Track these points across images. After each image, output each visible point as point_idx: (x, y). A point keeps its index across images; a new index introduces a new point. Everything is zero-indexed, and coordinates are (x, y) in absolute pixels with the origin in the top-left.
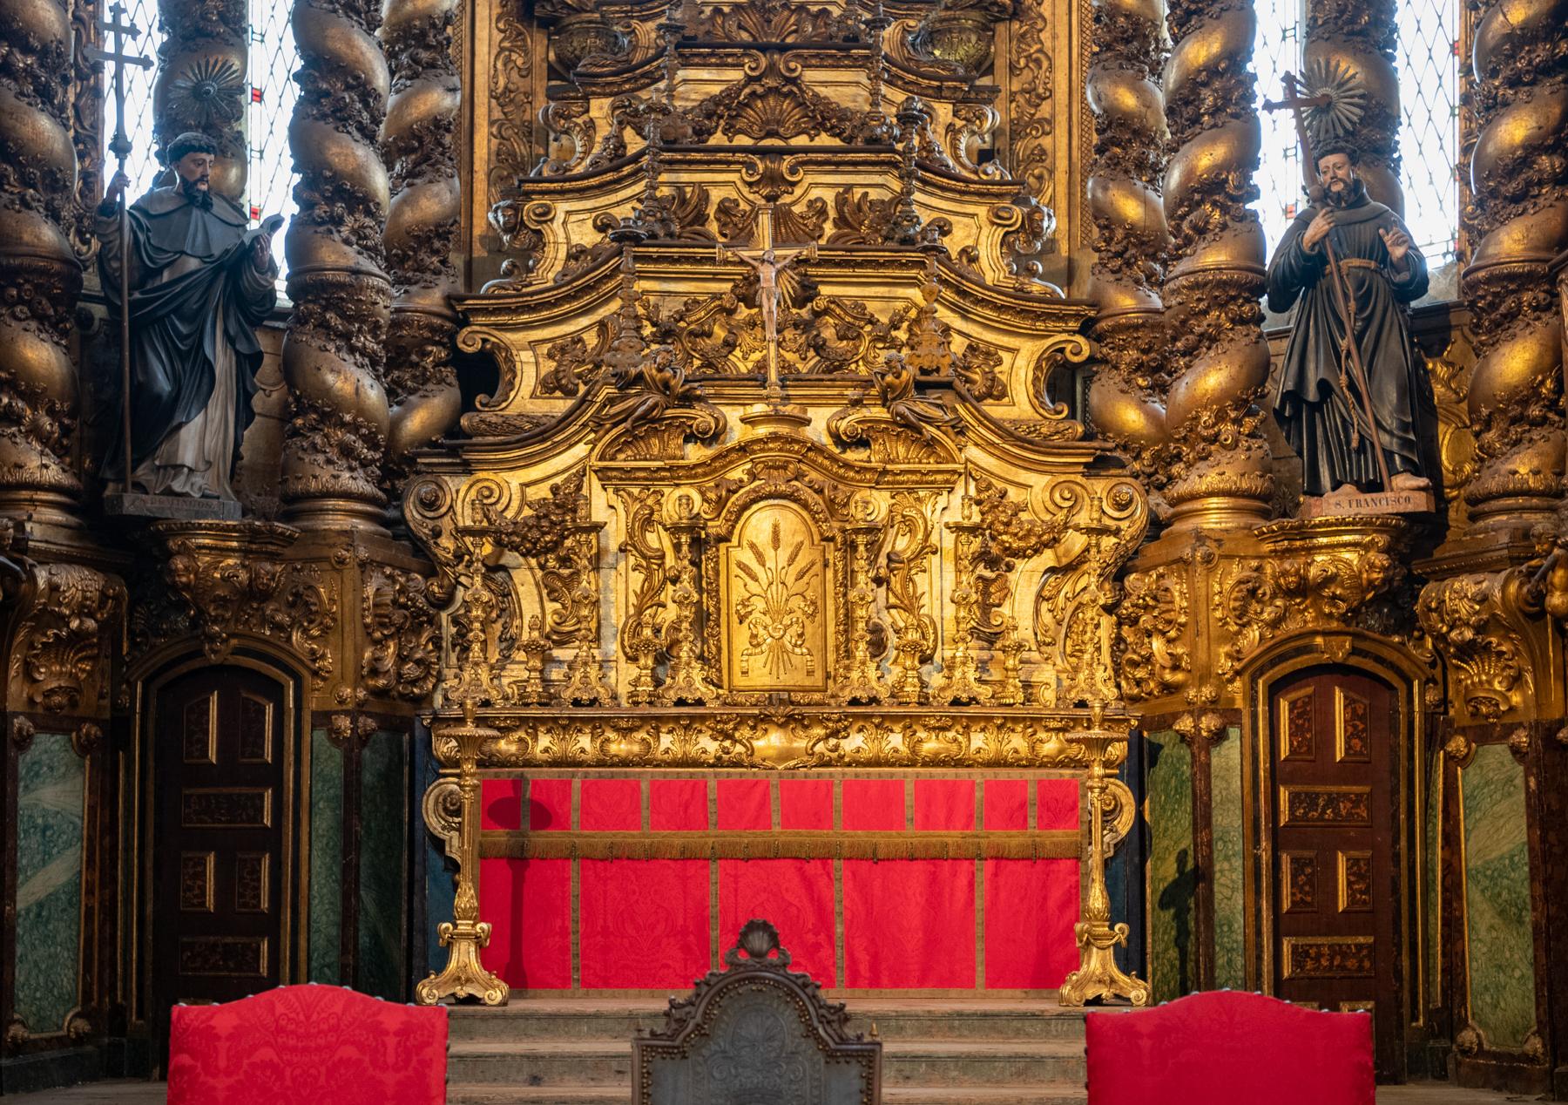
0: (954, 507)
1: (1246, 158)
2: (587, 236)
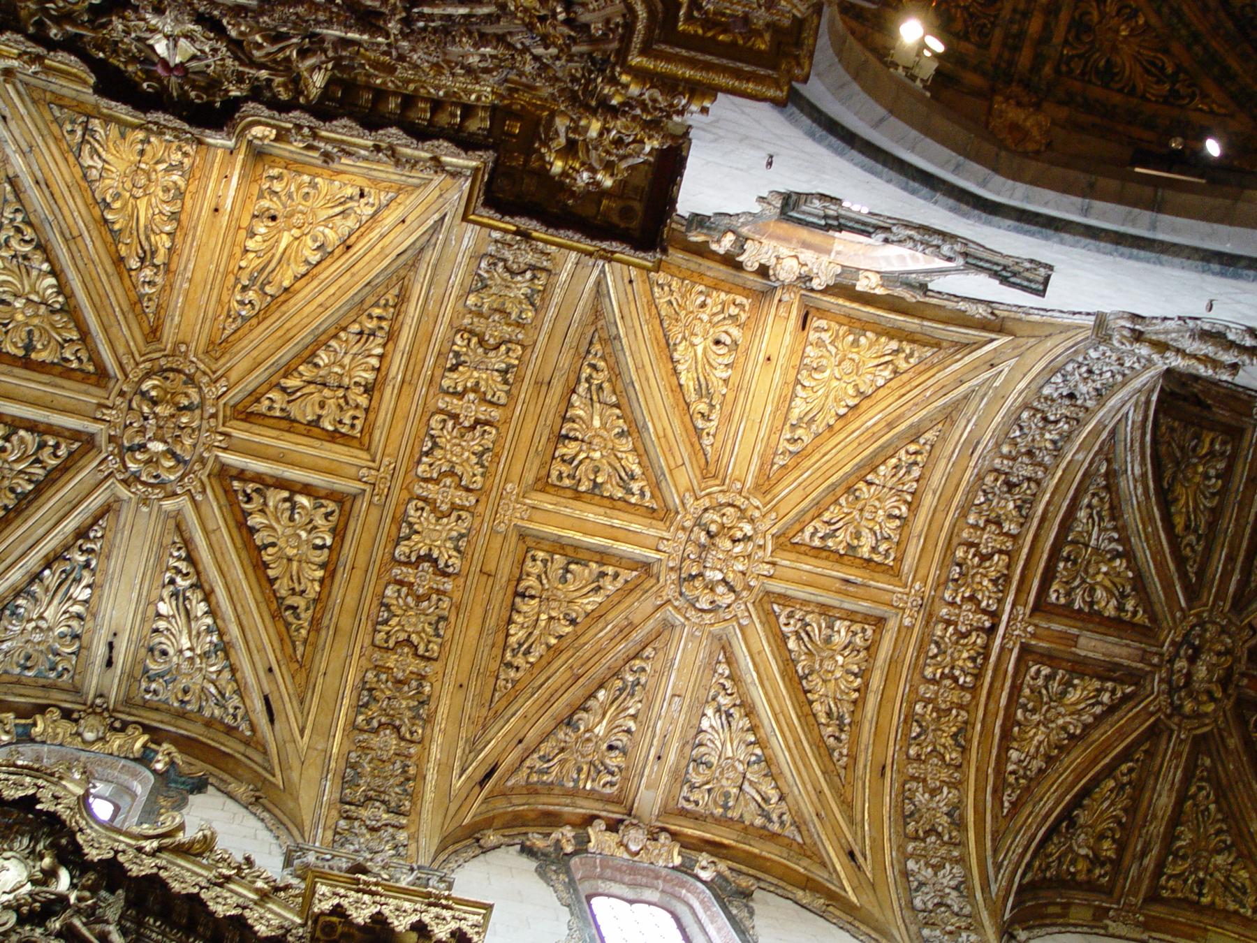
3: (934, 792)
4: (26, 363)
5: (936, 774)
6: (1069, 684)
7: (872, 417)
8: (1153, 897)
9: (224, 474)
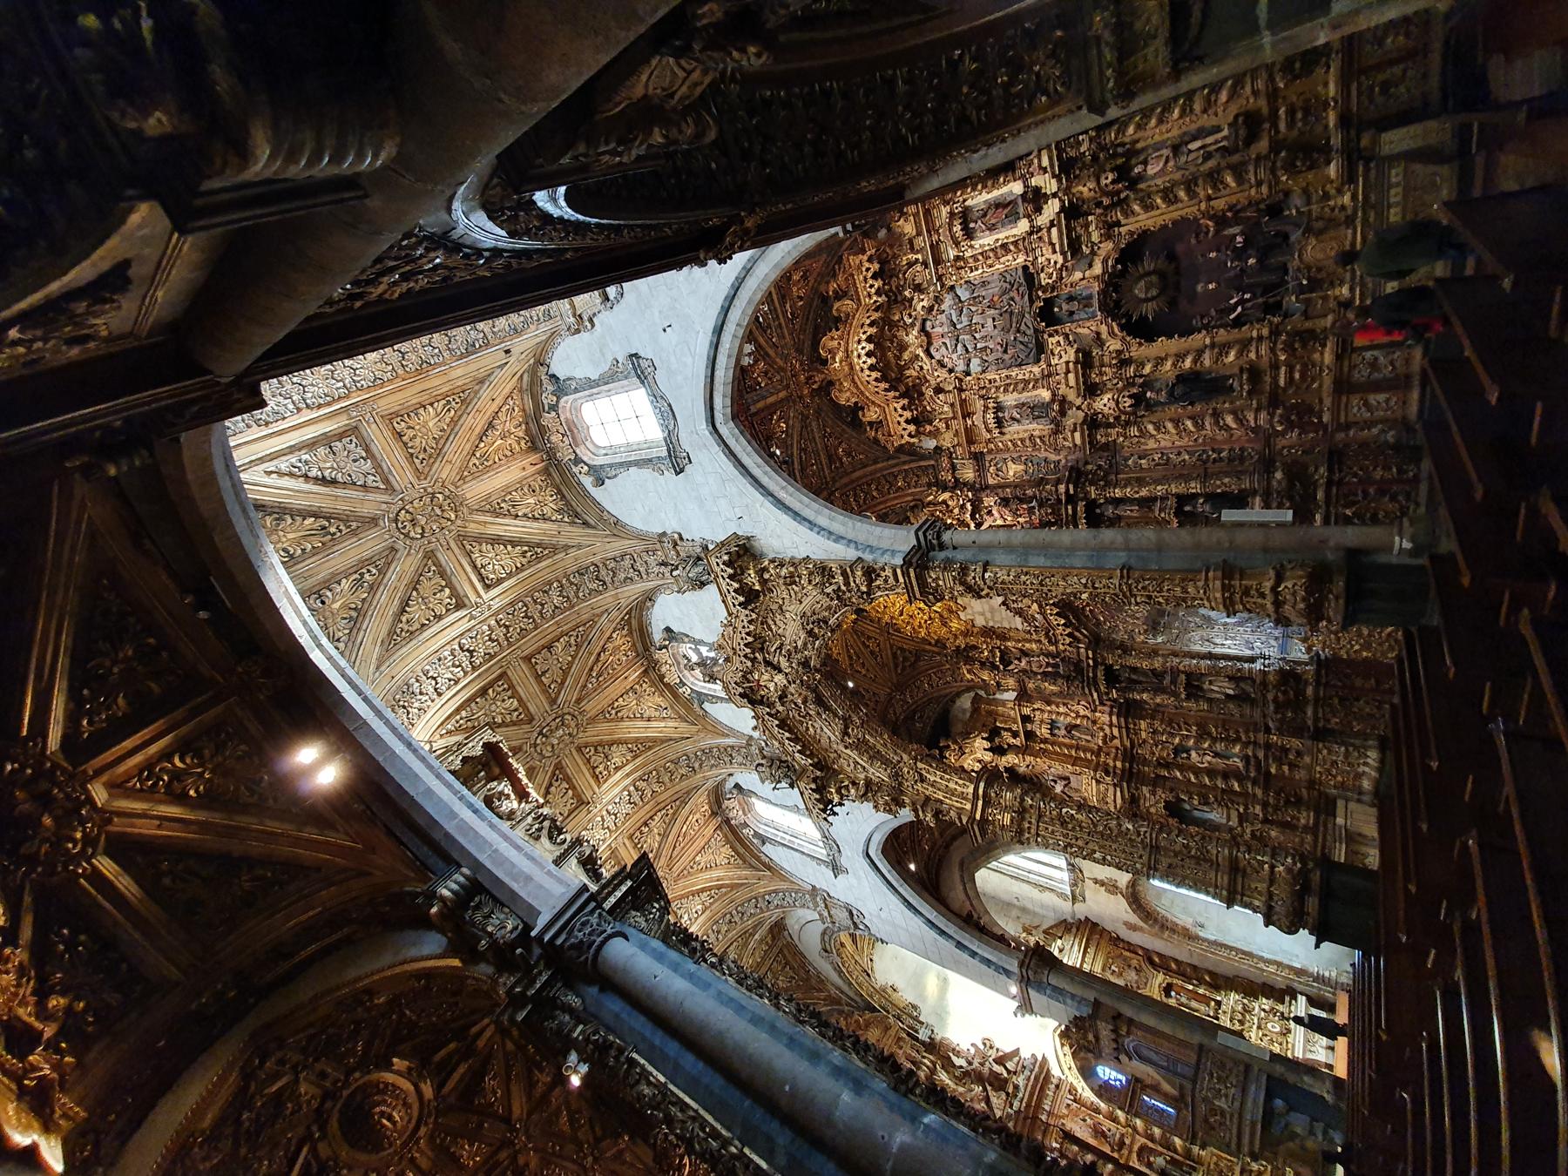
4: (538, 677)
7: (715, 874)
9: (559, 767)
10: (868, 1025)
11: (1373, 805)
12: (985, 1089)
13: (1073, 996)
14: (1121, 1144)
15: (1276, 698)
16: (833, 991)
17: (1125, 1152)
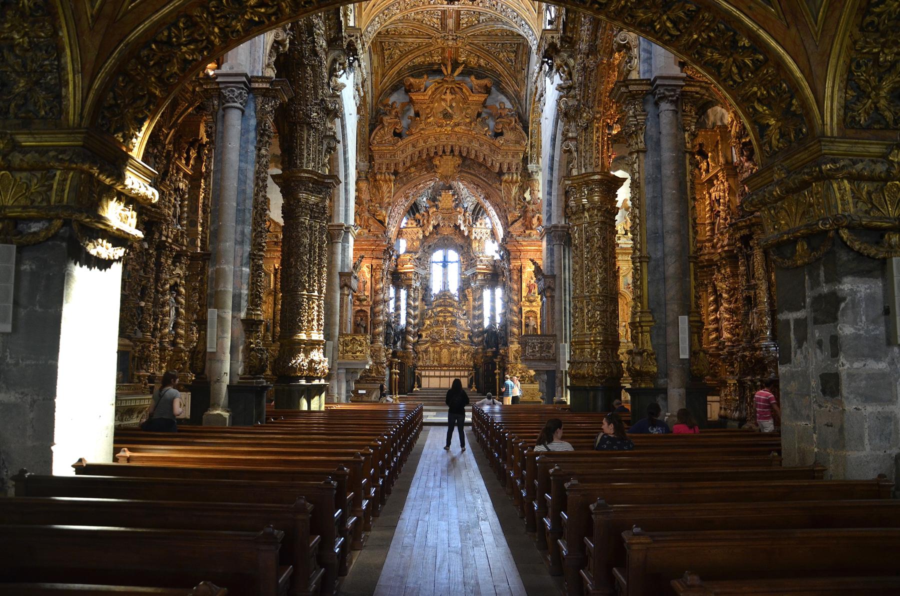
0: (459, 350)
1: (483, 321)
2: (429, 323)
3: (397, 9)
5: (402, 7)
6: (437, 18)
8: (381, 42)
10: (514, 129)
11: (720, 416)
12: (520, 217)
13: (552, 262)
14: (531, 302)
15: (746, 356)
16: (523, 93)
17: (528, 304)
